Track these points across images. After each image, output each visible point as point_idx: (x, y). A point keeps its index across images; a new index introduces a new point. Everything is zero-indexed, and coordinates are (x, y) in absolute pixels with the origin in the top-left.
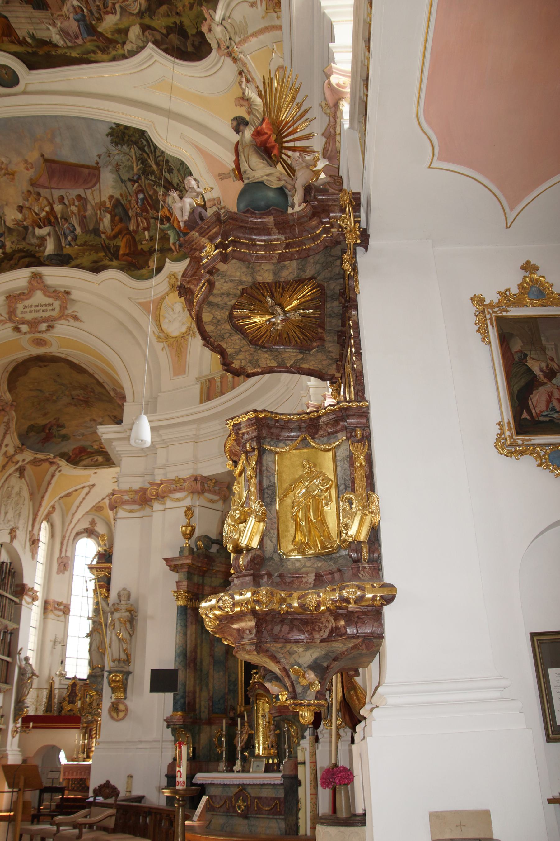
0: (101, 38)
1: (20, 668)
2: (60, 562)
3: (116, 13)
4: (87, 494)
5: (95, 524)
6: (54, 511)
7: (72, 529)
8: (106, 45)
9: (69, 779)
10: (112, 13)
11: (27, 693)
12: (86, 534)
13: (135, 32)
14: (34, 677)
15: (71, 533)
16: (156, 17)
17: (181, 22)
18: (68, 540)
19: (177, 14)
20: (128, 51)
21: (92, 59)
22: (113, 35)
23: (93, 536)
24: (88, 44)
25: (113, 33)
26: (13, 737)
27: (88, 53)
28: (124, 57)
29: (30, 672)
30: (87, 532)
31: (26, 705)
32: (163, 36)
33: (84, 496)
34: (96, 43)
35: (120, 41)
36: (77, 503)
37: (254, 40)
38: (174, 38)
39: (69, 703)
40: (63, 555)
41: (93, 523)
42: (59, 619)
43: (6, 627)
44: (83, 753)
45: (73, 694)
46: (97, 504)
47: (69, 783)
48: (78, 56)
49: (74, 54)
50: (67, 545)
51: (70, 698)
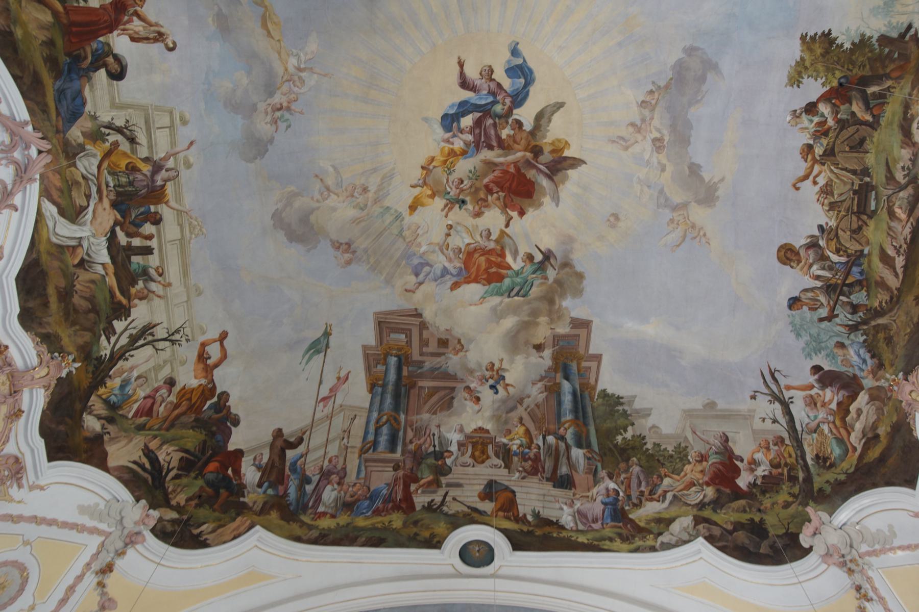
0: (629, 526)
3: (663, 501)
8: (633, 533)
10: (659, 501)
13: (684, 523)
16: (723, 511)
17: (762, 520)
19: (759, 510)
20: (662, 543)
21: (605, 547)
22: (647, 523)
24: (608, 530)
25: (648, 522)
27: (603, 539)
28: (653, 549)
32: (724, 532)
34: (619, 530)
35: (656, 531)
37: (900, 553)
38: (742, 537)
48: (586, 541)
49: (582, 539)
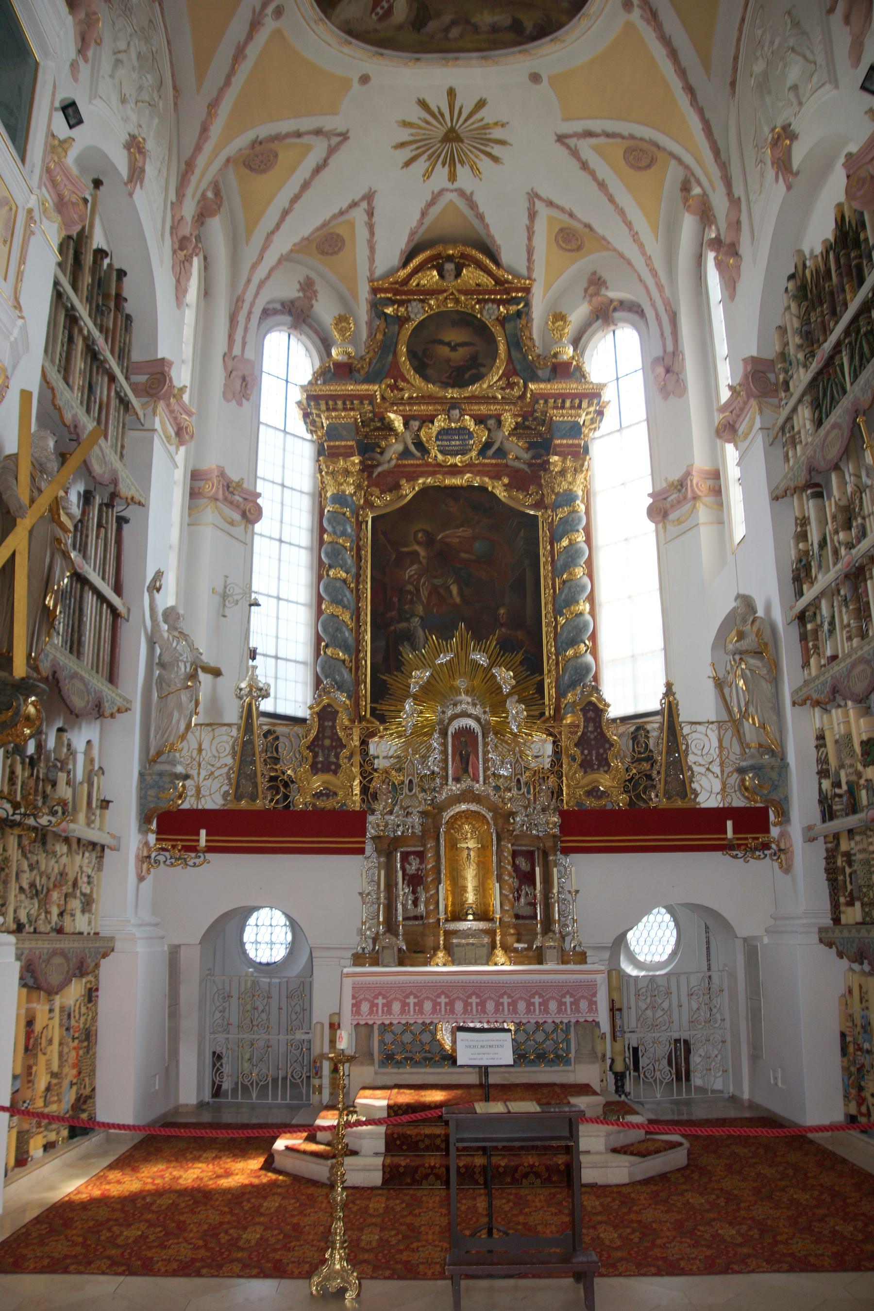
1: (151, 643)
2: (230, 369)
4: (318, 170)
5: (315, 292)
6: (219, 206)
7: (262, 283)
9: (369, 1027)
11: (182, 726)
12: (288, 319)
14: (202, 676)
15: (257, 293)
18: (250, 313)
23: (306, 328)
26: (141, 879)
29: (187, 656)
30: (290, 313)
31: (180, 769)
33: (308, 176)
36: (282, 199)
39: (315, 769)
40: (237, 350)
41: (308, 286)
42: (234, 530)
43: (115, 482)
44: (396, 935)
45: (327, 742)
46: (334, 217)
47: (370, 1037)
50: (246, 329)
51: (316, 756)
